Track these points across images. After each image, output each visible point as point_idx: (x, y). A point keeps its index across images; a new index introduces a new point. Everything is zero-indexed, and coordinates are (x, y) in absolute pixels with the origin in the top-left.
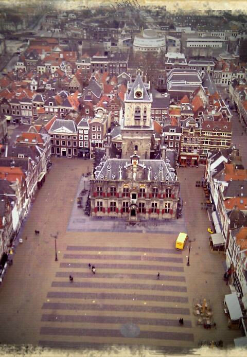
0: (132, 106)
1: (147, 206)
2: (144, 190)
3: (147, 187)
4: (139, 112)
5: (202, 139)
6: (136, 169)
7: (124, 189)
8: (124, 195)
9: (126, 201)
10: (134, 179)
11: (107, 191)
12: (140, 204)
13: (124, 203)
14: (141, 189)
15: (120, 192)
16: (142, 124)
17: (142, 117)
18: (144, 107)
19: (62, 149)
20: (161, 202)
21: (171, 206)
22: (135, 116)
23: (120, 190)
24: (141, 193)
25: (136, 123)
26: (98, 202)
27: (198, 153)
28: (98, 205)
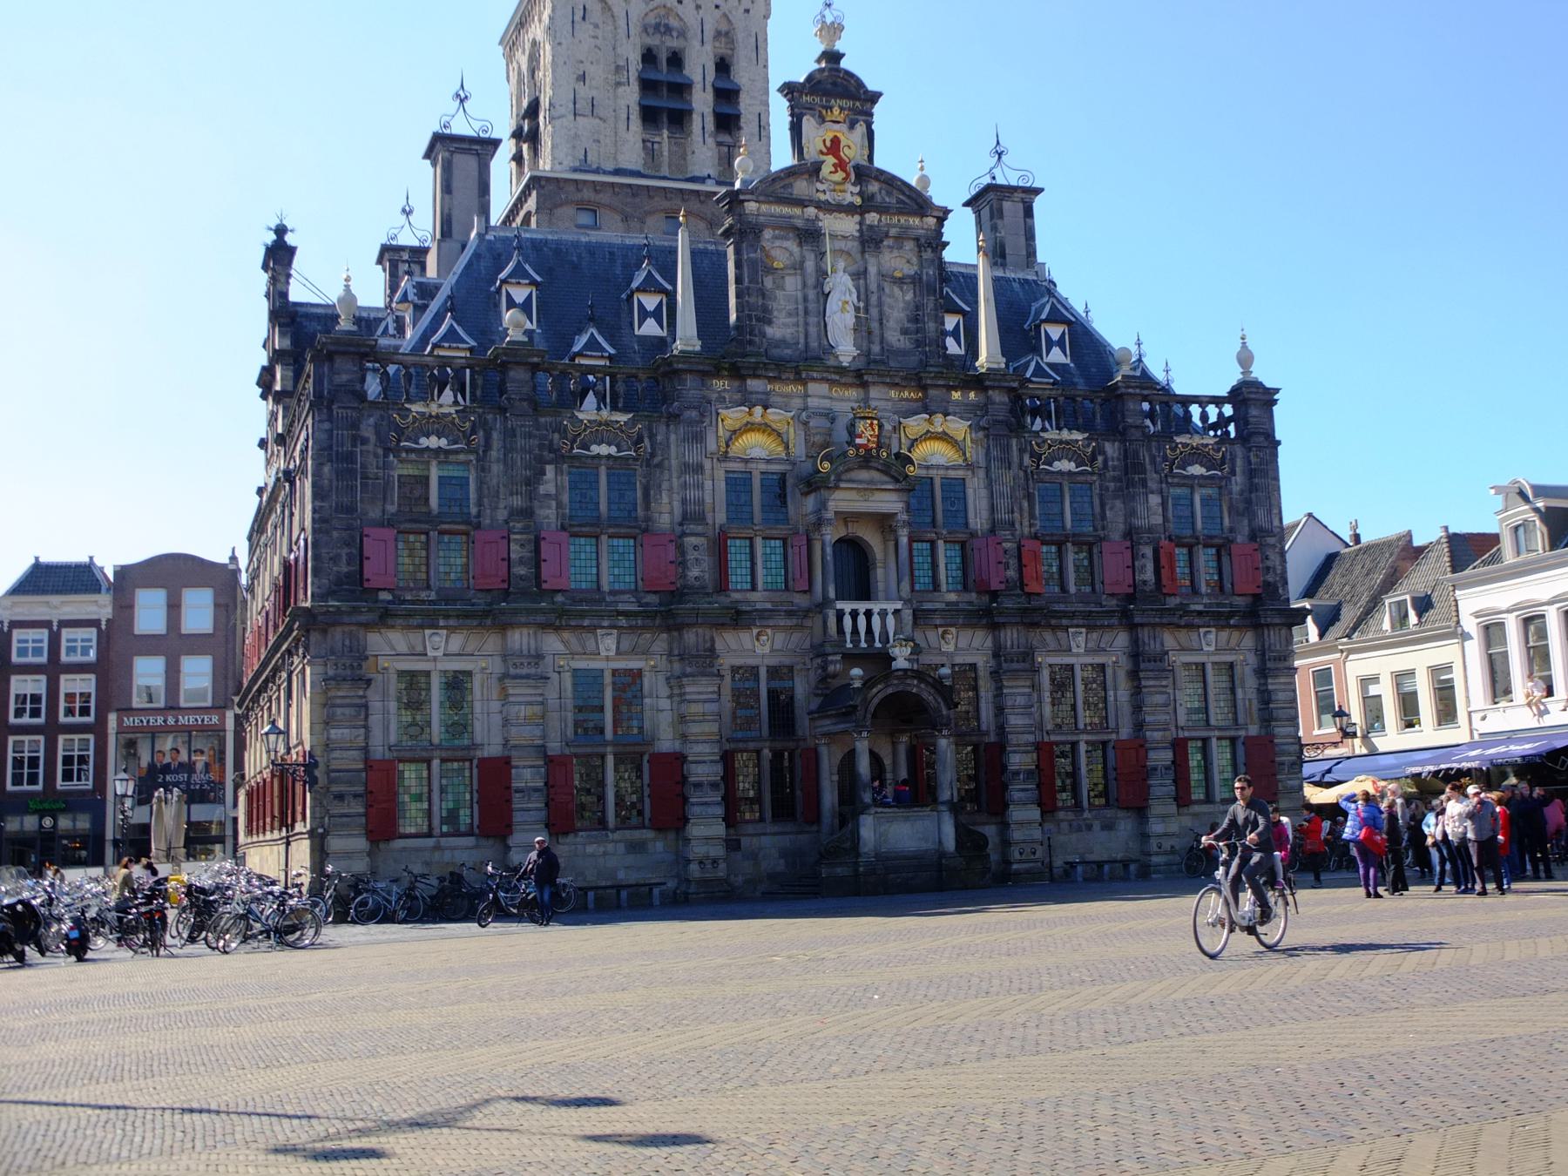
2: (956, 489)
3: (974, 453)
4: (676, 60)
6: (847, 225)
7: (738, 485)
15: (692, 516)
17: (702, 102)
22: (647, 86)
25: (650, 151)
26: (414, 682)
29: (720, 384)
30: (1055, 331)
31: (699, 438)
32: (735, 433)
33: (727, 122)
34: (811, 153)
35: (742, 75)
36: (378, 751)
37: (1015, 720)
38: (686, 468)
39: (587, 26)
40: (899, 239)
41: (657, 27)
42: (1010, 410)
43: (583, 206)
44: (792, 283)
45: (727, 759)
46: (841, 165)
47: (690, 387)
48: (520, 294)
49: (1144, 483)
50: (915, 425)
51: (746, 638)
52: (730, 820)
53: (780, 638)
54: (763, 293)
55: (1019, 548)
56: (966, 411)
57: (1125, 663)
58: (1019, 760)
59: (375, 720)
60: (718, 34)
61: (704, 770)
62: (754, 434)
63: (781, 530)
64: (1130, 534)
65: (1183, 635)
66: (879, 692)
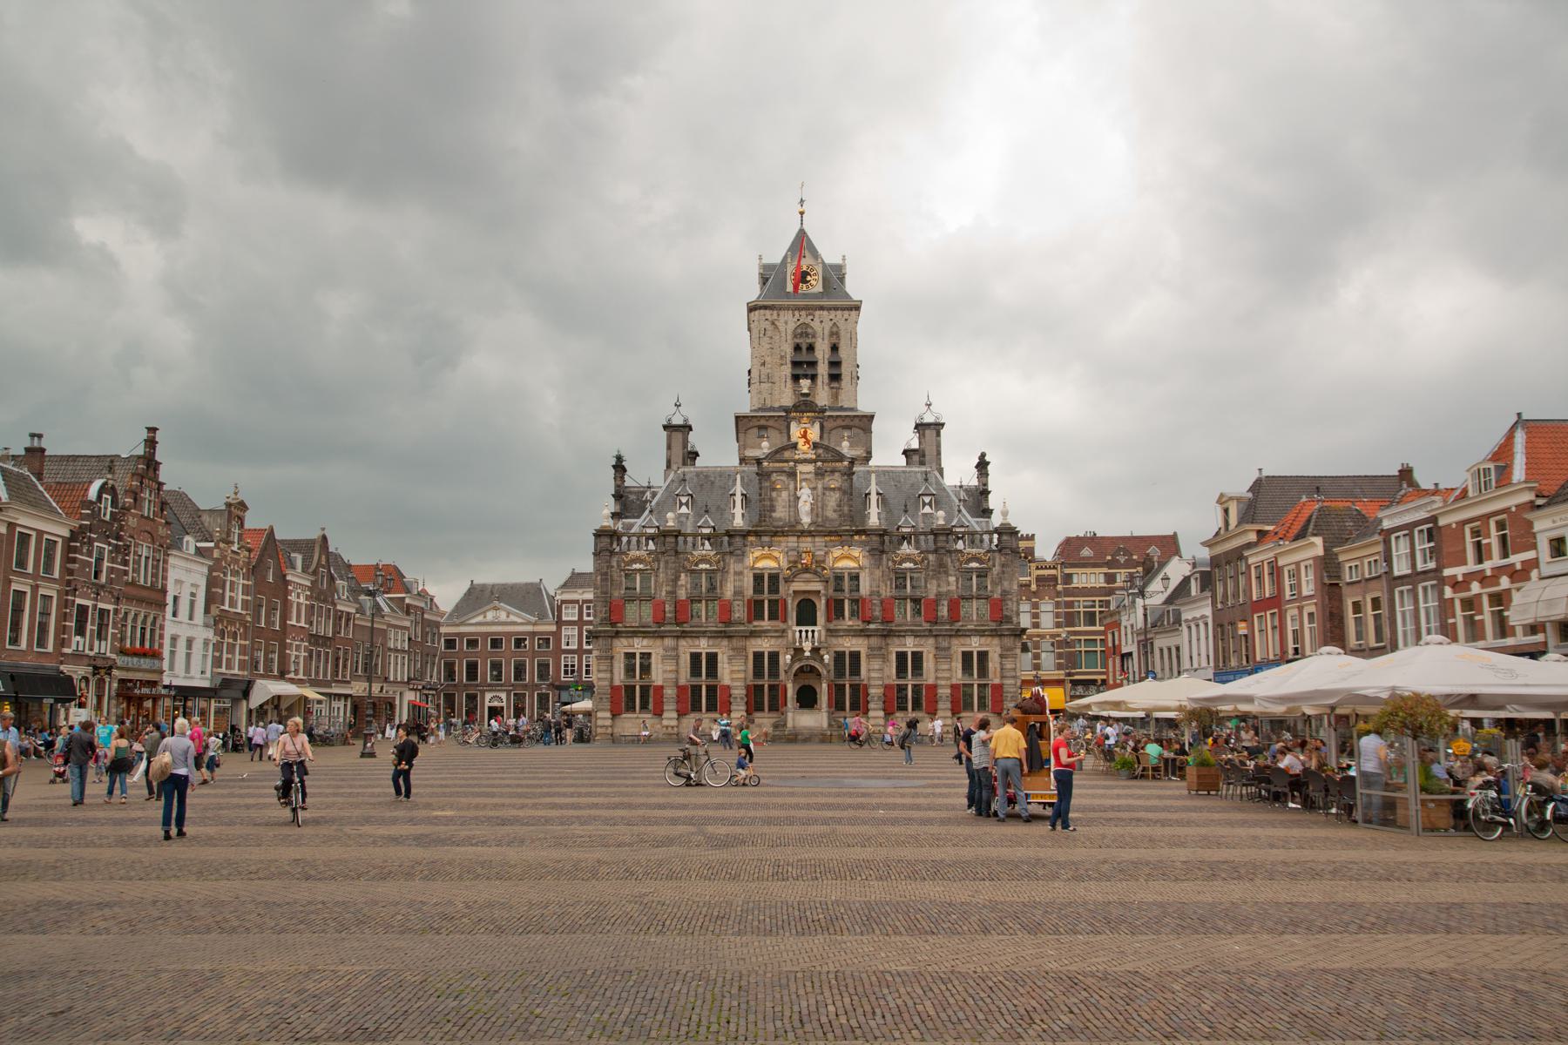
0: (781, 325)
1: (876, 664)
4: (811, 348)
5: (1070, 604)
6: (810, 468)
7: (758, 578)
8: (755, 609)
9: (765, 645)
10: (806, 520)
11: (673, 593)
12: (839, 657)
13: (758, 656)
14: (839, 578)
15: (738, 593)
16: (822, 397)
17: (823, 370)
18: (828, 326)
19: (488, 696)
20: (942, 654)
21: (993, 664)
22: (795, 364)
23: (737, 584)
24: (841, 598)
27: (1059, 667)
28: (630, 670)
29: (751, 538)
30: (927, 499)
31: (741, 561)
32: (757, 559)
33: (835, 377)
34: (794, 439)
35: (843, 353)
36: (617, 683)
37: (873, 675)
38: (736, 573)
39: (766, 339)
40: (833, 472)
41: (801, 335)
42: (882, 542)
43: (761, 428)
44: (784, 494)
45: (748, 688)
46: (807, 442)
47: (738, 541)
48: (684, 500)
49: (946, 573)
50: (837, 552)
51: (759, 641)
52: (748, 712)
53: (773, 641)
54: (771, 500)
55: (882, 602)
56: (862, 544)
57: (933, 651)
58: (872, 691)
59: (616, 671)
60: (832, 334)
61: (739, 692)
62: (766, 559)
63: (774, 597)
64: (939, 594)
65: (962, 640)
66: (797, 666)
